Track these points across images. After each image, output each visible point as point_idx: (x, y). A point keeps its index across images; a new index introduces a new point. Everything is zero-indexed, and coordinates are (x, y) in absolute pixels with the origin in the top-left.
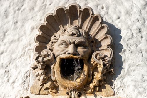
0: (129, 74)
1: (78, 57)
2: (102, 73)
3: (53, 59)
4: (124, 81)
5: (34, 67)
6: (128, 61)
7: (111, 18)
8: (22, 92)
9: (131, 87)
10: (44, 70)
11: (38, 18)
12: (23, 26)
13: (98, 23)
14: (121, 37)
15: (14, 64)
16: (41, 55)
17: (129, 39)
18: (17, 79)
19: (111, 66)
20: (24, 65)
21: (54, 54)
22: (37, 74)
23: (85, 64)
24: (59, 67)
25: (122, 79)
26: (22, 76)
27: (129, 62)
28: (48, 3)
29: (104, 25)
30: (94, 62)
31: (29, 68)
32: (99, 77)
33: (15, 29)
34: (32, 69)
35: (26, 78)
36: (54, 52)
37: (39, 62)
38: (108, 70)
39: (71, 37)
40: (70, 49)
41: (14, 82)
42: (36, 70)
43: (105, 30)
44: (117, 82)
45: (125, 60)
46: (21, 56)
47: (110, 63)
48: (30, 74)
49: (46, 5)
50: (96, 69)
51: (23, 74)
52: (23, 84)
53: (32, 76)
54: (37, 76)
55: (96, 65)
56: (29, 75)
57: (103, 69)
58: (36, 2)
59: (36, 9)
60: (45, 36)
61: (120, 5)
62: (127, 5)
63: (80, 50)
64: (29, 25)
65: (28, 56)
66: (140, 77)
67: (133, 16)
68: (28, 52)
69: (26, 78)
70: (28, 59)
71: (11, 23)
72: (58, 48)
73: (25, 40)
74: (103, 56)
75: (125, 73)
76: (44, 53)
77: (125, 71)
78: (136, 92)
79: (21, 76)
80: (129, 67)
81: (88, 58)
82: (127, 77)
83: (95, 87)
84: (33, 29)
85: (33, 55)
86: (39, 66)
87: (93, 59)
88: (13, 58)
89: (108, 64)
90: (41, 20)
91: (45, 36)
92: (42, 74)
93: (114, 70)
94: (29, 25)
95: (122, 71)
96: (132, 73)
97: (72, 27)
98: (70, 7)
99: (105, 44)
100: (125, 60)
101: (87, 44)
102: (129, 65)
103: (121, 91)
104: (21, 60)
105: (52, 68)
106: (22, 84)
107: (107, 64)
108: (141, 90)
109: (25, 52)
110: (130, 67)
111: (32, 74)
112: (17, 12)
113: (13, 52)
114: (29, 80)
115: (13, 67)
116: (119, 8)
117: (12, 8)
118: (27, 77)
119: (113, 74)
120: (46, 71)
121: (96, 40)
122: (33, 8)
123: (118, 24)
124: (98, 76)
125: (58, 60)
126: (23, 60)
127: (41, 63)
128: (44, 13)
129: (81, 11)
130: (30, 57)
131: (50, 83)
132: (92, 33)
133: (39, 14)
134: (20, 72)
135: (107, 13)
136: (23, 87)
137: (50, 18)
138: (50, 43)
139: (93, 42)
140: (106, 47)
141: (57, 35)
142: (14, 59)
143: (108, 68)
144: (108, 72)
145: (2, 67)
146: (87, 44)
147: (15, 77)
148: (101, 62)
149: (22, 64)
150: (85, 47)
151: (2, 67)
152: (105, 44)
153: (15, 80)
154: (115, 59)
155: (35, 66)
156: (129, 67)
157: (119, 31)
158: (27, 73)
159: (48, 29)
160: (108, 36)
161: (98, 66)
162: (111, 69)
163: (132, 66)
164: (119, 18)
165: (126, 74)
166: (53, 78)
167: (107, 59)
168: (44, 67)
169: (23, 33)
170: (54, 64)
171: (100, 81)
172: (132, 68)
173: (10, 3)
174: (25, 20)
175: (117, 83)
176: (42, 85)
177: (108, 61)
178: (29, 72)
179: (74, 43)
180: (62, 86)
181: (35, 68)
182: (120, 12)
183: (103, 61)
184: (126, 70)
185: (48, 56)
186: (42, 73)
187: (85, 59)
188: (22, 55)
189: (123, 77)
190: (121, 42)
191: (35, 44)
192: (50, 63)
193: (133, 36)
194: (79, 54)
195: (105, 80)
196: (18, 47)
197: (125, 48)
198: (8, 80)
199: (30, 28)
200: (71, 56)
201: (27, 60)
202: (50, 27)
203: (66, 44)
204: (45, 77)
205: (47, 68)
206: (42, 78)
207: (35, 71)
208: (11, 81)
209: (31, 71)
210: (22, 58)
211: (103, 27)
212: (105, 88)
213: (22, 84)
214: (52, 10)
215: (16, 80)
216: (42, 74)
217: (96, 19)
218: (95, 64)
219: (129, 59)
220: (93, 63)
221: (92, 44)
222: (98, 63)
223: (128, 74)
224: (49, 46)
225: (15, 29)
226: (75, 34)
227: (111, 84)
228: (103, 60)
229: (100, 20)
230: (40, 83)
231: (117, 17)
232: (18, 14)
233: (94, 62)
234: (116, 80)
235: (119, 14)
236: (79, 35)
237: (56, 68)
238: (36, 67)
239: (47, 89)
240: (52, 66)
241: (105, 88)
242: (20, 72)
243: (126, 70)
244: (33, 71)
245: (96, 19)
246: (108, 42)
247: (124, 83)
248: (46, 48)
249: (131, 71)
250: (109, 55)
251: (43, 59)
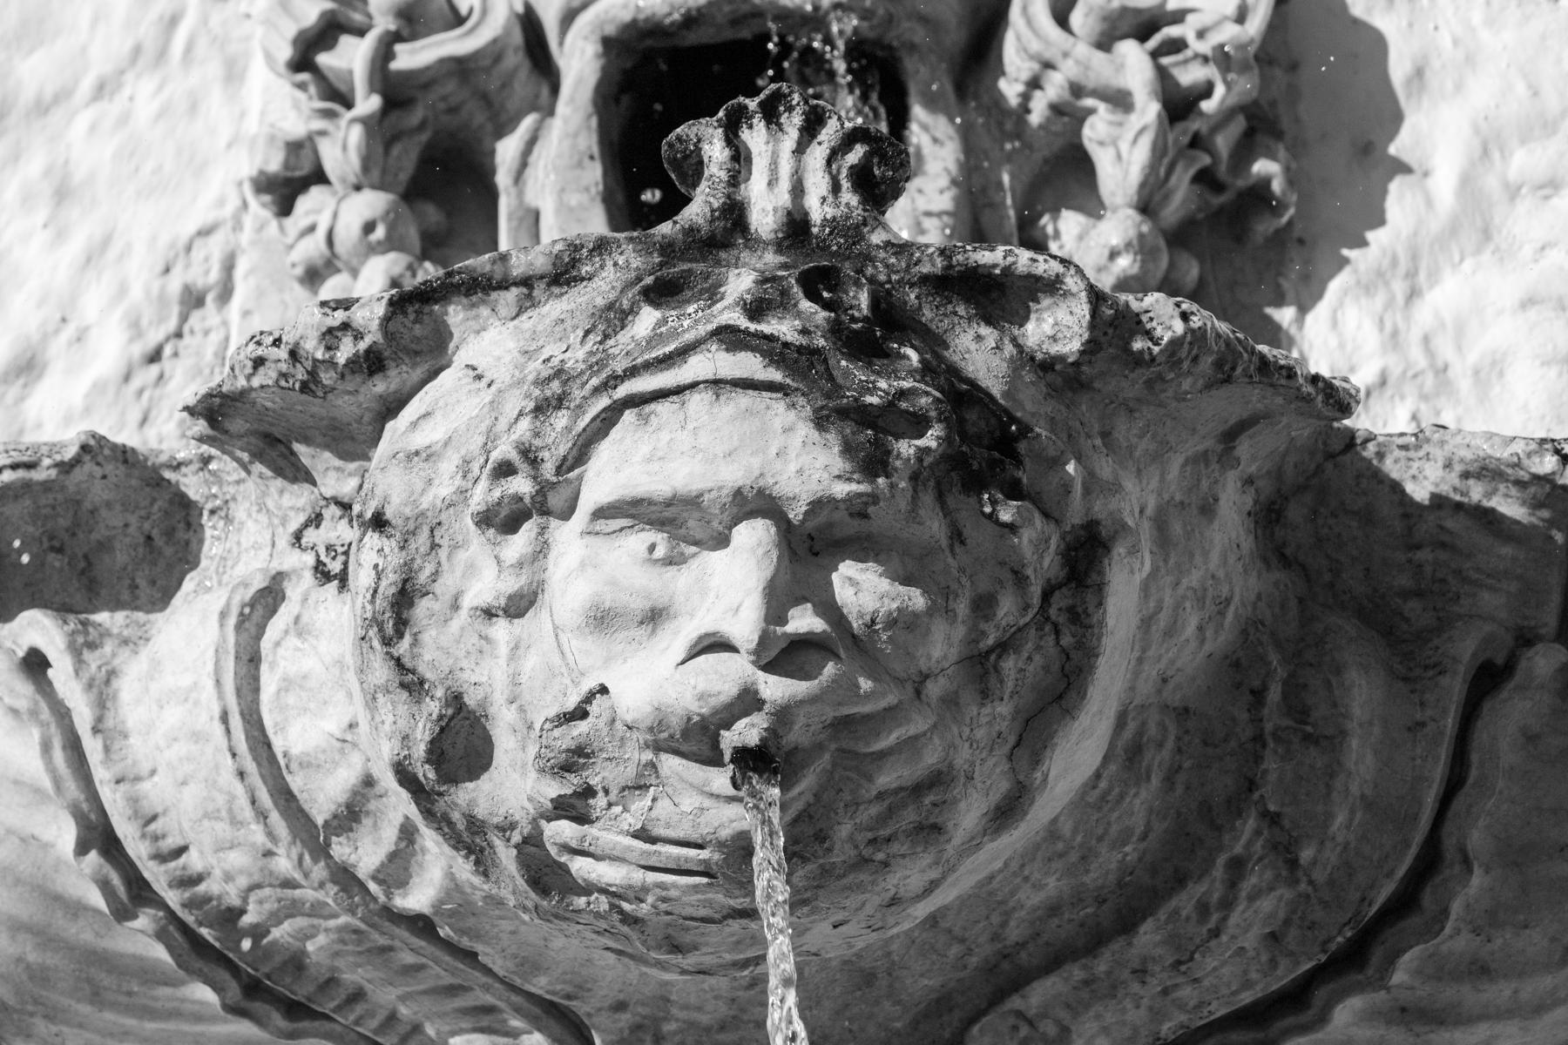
0: (1486, 234)
2: (1146, 206)
3: (515, 59)
4: (1423, 314)
5: (275, 164)
6: (1459, 87)
10: (413, 194)
15: (34, 166)
16: (357, 17)
18: (69, 331)
20: (158, 169)
22: (313, 247)
23: (932, 103)
24: (589, 141)
25: (1399, 288)
26: (136, 293)
27: (1482, 93)
30: (1035, 84)
31: (221, 202)
32: (1113, 255)
34: (259, 209)
35: (184, 318)
37: (337, 95)
38: (1222, 171)
42: (311, 203)
45: (1419, 73)
46: (122, 72)
47: (1246, 85)
48: (229, 267)
51: (139, 273)
52: (136, 382)
53: (260, 293)
55: (1069, 114)
56: (215, 275)
57: (1158, 150)
65: (214, 69)
68: (215, 20)
69: (184, 318)
70: (215, 99)
75: (1435, 225)
77: (1429, 202)
79: (122, 290)
80: (1485, 152)
81: (956, 36)
82: (1468, 265)
88: (27, 95)
89: (1220, 90)
92: (380, 232)
93: (1291, 180)
95: (1399, 200)
100: (1419, 73)
102: (1476, 130)
104: (124, 119)
105: (503, 179)
106: (127, 378)
107: (1207, 91)
109: (173, 21)
111: (251, 272)
114: (215, 338)
115: (27, 199)
118: (193, 300)
119: (1280, 239)
120: (433, 214)
126: (145, 109)
127: (367, 104)
130: (233, 74)
134: (106, 242)
136: (134, 415)
142: (42, 108)
143: (1223, 143)
144: (1218, 200)
147: (41, 303)
153: (45, 338)
154: (1293, 67)
155: (295, 148)
156: (1485, 152)
158: (198, 254)
161: (1097, 129)
162: (1263, 167)
163: (1523, 141)
165: (1453, 229)
167: (1201, 34)
168: (407, 158)
170: (528, 122)
175: (1342, 346)
177: (1222, 59)
178: (215, 247)
183: (1155, 55)
184: (1444, 182)
186: (369, 227)
187: (919, 35)
188: (137, 51)
189: (1411, 274)
192: (480, 118)
201: (193, 108)
204: (412, 269)
207: (289, 222)
209: (246, 237)
210: (143, 93)
213: (127, 378)
215: (57, 348)
216: (380, 232)
218: (1057, 109)
219: (1470, 60)
220: (1026, 97)
222: (1091, 82)
228: (1154, 42)
233: (1035, 84)
234: (1318, 316)
238: (305, 169)
240: (507, 150)
242: (106, 242)
243: (1444, 182)
244: (274, 224)
247: (1426, 340)
249: (1513, 192)
251: (385, 52)
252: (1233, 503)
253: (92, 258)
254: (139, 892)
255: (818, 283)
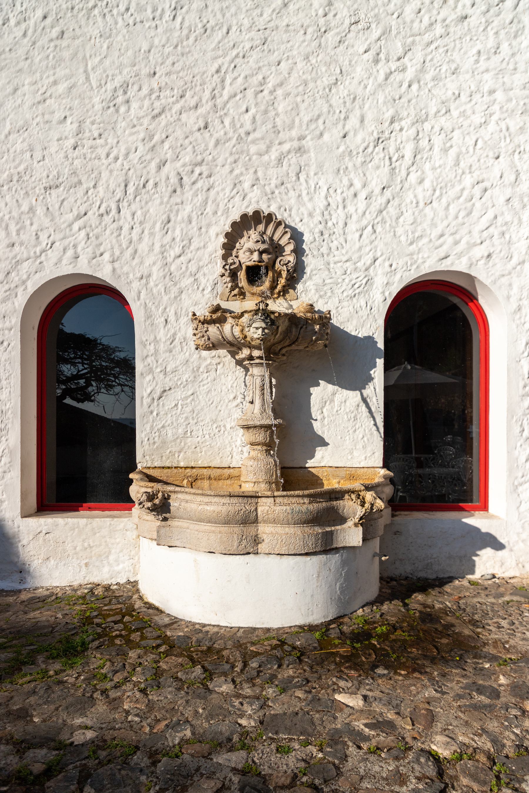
1: (263, 264)
7: (294, 222)
8: (211, 299)
9: (313, 291)
11: (222, 222)
12: (207, 232)
13: (281, 228)
14: (304, 241)
17: (312, 243)
19: (295, 271)
21: (239, 261)
22: (224, 281)
28: (231, 206)
29: (287, 230)
33: (200, 235)
36: (240, 258)
37: (226, 270)
39: (256, 244)
40: (255, 256)
41: (203, 290)
43: (288, 236)
44: (300, 287)
49: (228, 208)
50: (279, 274)
51: (211, 281)
54: (225, 283)
55: (280, 271)
58: (218, 205)
59: (219, 213)
60: (230, 242)
61: (303, 206)
62: (309, 205)
63: (265, 257)
64: (213, 230)
66: (320, 281)
67: (315, 218)
71: (195, 229)
72: (244, 256)
73: (210, 248)
74: (286, 262)
76: (230, 261)
78: (317, 296)
83: (279, 292)
84: (217, 235)
85: (220, 263)
86: (227, 274)
87: (277, 265)
90: (224, 225)
91: (230, 242)
94: (213, 230)
95: (305, 276)
96: (314, 278)
97: (257, 234)
98: (254, 213)
99: (289, 248)
101: (271, 250)
103: (303, 295)
108: (322, 293)
110: (312, 271)
112: (200, 217)
113: (200, 260)
116: (302, 209)
117: (194, 213)
121: (280, 245)
122: (216, 213)
123: (300, 228)
124: (282, 281)
125: (244, 267)
128: (227, 217)
129: (264, 217)
130: (216, 264)
131: (237, 290)
132: (276, 238)
133: (223, 219)
135: (290, 215)
137: (234, 225)
138: (235, 250)
139: (276, 247)
140: (289, 253)
141: (242, 241)
145: (191, 275)
146: (271, 250)
148: (285, 268)
149: (209, 271)
150: (269, 253)
151: (191, 275)
152: (289, 248)
157: (302, 235)
159: (233, 235)
160: (291, 241)
161: (282, 272)
164: (301, 221)
166: (240, 285)
169: (208, 239)
171: (284, 286)
172: (314, 272)
173: (192, 208)
174: (209, 225)
176: (231, 292)
179: (259, 250)
180: (249, 292)
181: (222, 276)
182: (303, 214)
184: (308, 274)
185: (234, 263)
190: (304, 246)
191: (221, 252)
193: (315, 240)
194: (264, 261)
195: (288, 285)
196: (204, 254)
197: (307, 252)
198: (198, 288)
199: (215, 233)
200: (257, 263)
202: (234, 234)
203: (251, 252)
205: (234, 275)
206: (230, 285)
208: (201, 289)
211: (286, 232)
212: (288, 293)
214: (236, 216)
217: (279, 224)
221: (276, 250)
223: (310, 278)
224: (234, 253)
225: (200, 235)
226: (259, 241)
227: (294, 289)
229: (283, 225)
230: (228, 290)
231: (299, 220)
232: (202, 218)
235: (301, 216)
236: (264, 242)
237: (242, 275)
239: (235, 295)
240: (239, 273)
241: (288, 293)
243: (308, 274)
245: (279, 224)
246: (291, 247)
248: (232, 256)
250: (292, 261)
252: (287, 320)
253: (207, 281)
254: (225, 340)
255: (264, 314)
